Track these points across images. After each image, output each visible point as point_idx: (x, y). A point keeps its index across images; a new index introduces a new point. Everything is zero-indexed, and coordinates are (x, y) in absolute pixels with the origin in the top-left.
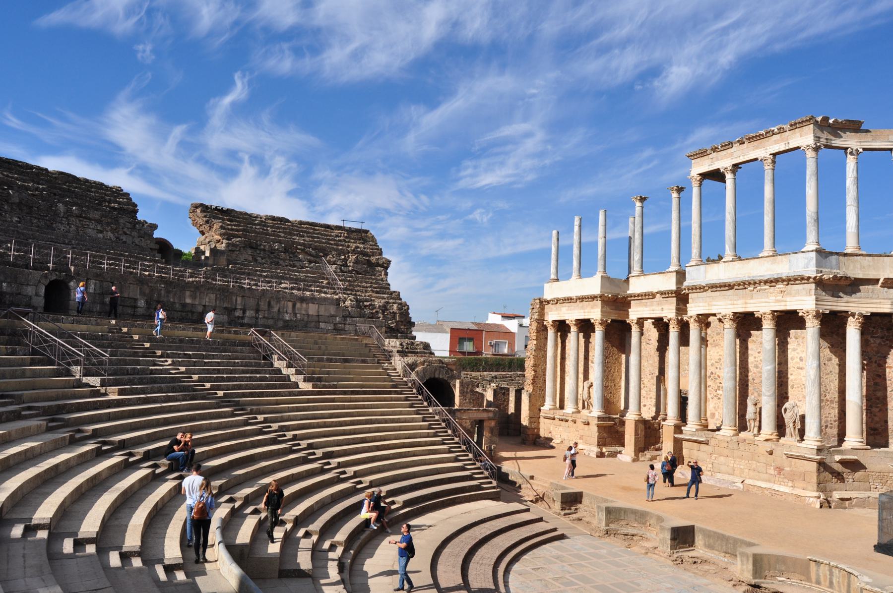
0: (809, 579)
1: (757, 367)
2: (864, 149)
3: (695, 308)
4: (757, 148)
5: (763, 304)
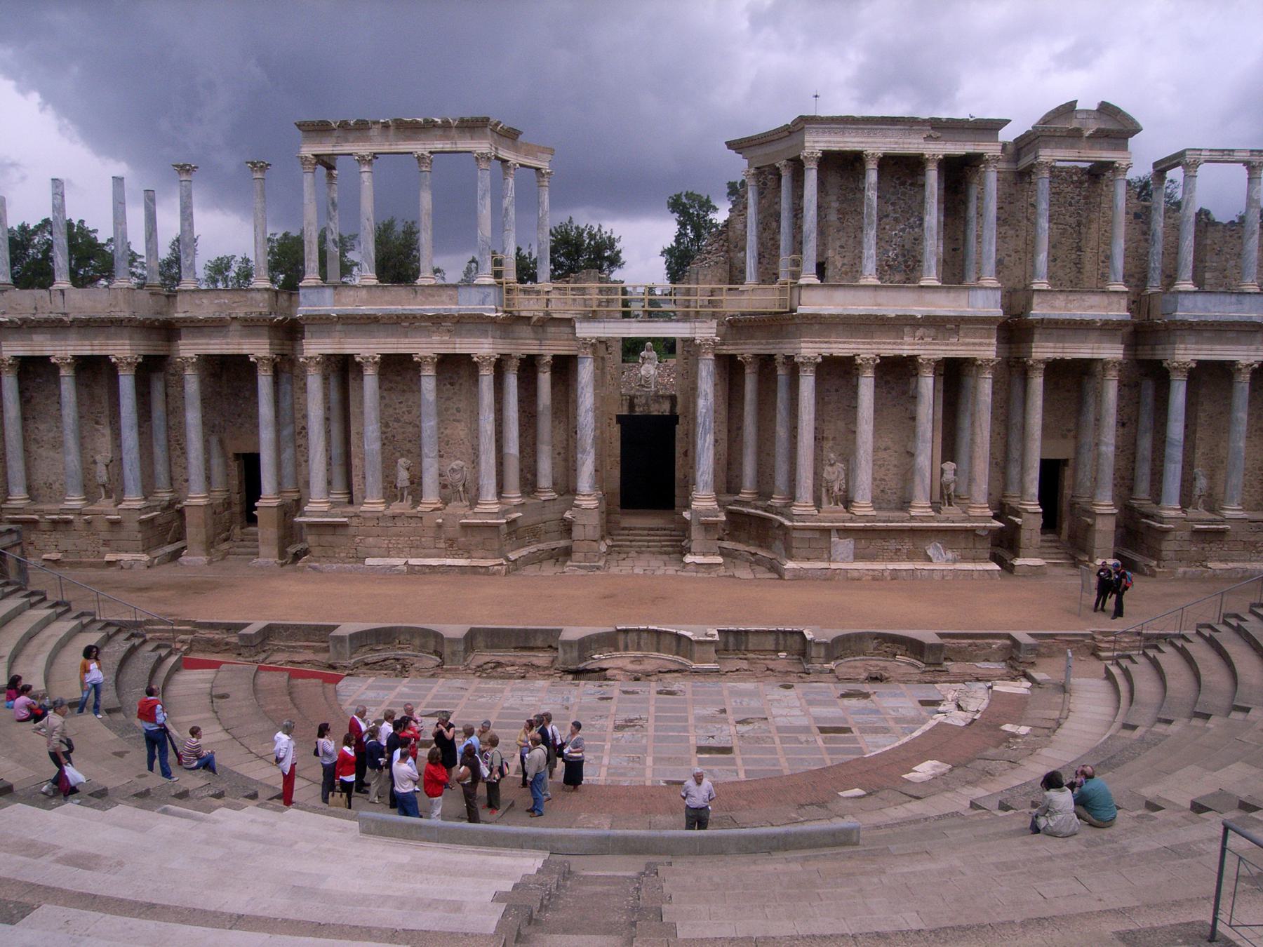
0: (617, 650)
1: (397, 420)
2: (521, 165)
3: (314, 347)
4: (409, 139)
5: (425, 347)
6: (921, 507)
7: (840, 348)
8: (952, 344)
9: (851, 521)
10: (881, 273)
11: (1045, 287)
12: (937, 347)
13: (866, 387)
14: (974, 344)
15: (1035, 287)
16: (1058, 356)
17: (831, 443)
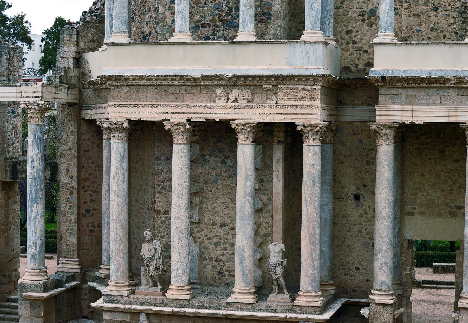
6: (241, 292)
7: (148, 112)
8: (270, 107)
9: (163, 304)
10: (196, 27)
11: (388, 40)
12: (253, 111)
13: (180, 153)
14: (295, 107)
15: (376, 41)
16: (407, 120)
17: (162, 218)
